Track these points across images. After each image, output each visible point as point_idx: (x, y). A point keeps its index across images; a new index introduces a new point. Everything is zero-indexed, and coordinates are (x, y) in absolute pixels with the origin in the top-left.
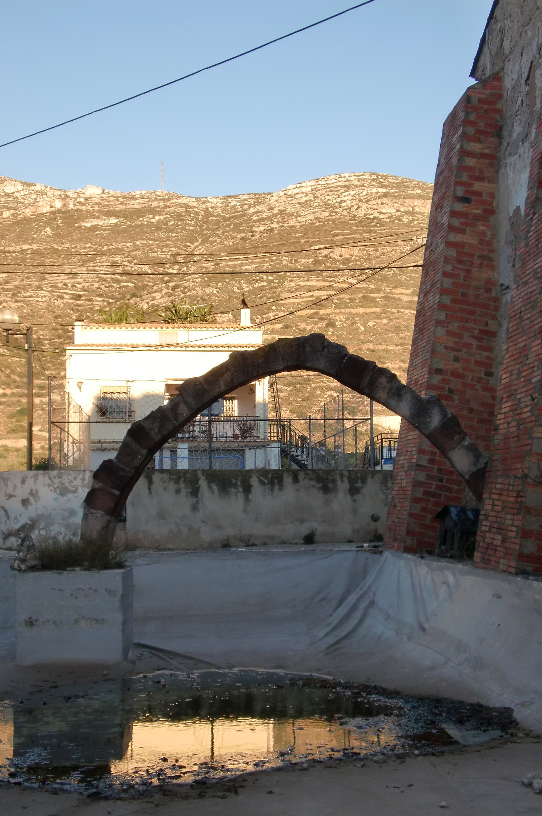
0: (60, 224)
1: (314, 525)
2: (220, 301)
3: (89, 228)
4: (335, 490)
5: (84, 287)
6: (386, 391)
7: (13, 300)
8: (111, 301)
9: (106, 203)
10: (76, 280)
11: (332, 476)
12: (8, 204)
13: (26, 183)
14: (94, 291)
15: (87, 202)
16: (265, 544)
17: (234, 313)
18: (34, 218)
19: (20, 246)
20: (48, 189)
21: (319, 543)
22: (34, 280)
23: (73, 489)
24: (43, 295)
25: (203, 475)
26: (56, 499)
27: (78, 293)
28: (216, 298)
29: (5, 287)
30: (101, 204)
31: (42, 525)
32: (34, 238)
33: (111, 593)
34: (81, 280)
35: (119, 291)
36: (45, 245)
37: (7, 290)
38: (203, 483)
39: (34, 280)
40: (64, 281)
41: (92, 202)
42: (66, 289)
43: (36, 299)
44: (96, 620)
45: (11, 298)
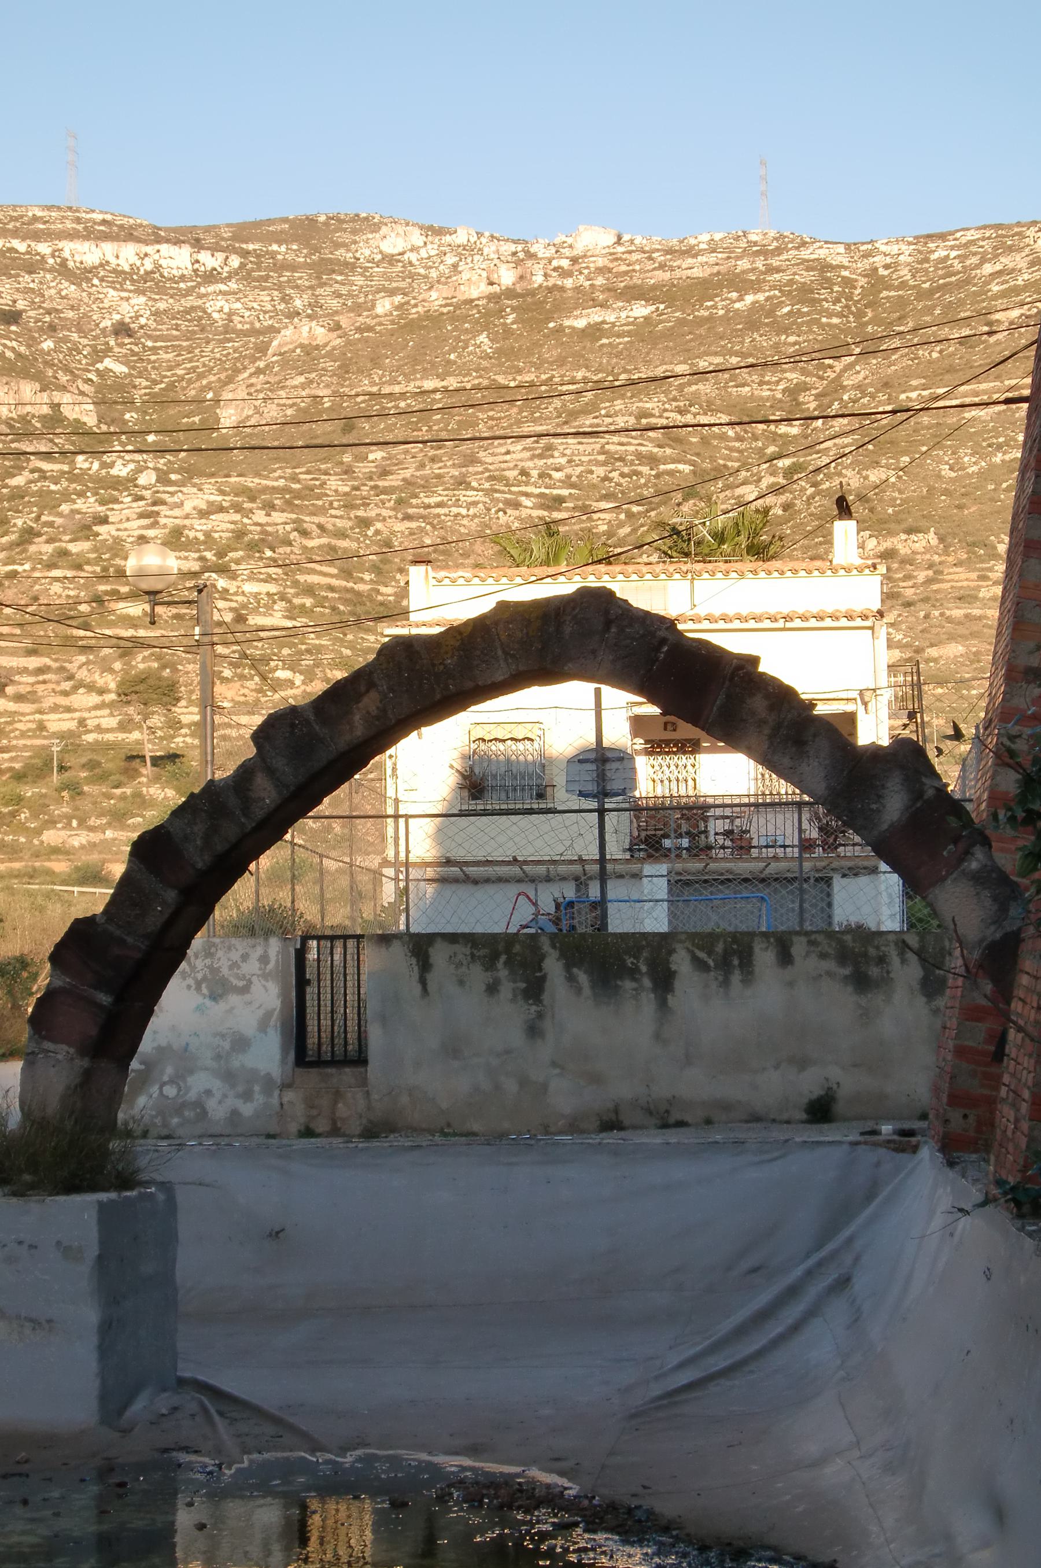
0: (513, 323)
1: (835, 1073)
2: (904, 501)
3: (583, 330)
4: (886, 982)
5: (569, 477)
6: (767, 731)
7: (400, 516)
8: (635, 509)
9: (624, 268)
10: (551, 461)
11: (877, 948)
12: (390, 280)
13: (431, 228)
14: (594, 486)
15: (577, 267)
16: (708, 1122)
17: (942, 531)
18: (449, 312)
19: (418, 383)
20: (484, 240)
21: (846, 1119)
22: (449, 463)
23: (241, 984)
24: (469, 500)
25: (554, 947)
26: (200, 1009)
27: (555, 492)
28: (896, 494)
29: (381, 483)
30: (610, 270)
31: (169, 1070)
32: (449, 362)
33: (68, 1252)
34: (563, 461)
35: (655, 485)
36: (477, 377)
37: (385, 491)
38: (553, 966)
39: (449, 463)
40: (521, 464)
41: (587, 268)
42: (527, 484)
43: (455, 510)
44: (31, 1320)
45: (393, 509)
